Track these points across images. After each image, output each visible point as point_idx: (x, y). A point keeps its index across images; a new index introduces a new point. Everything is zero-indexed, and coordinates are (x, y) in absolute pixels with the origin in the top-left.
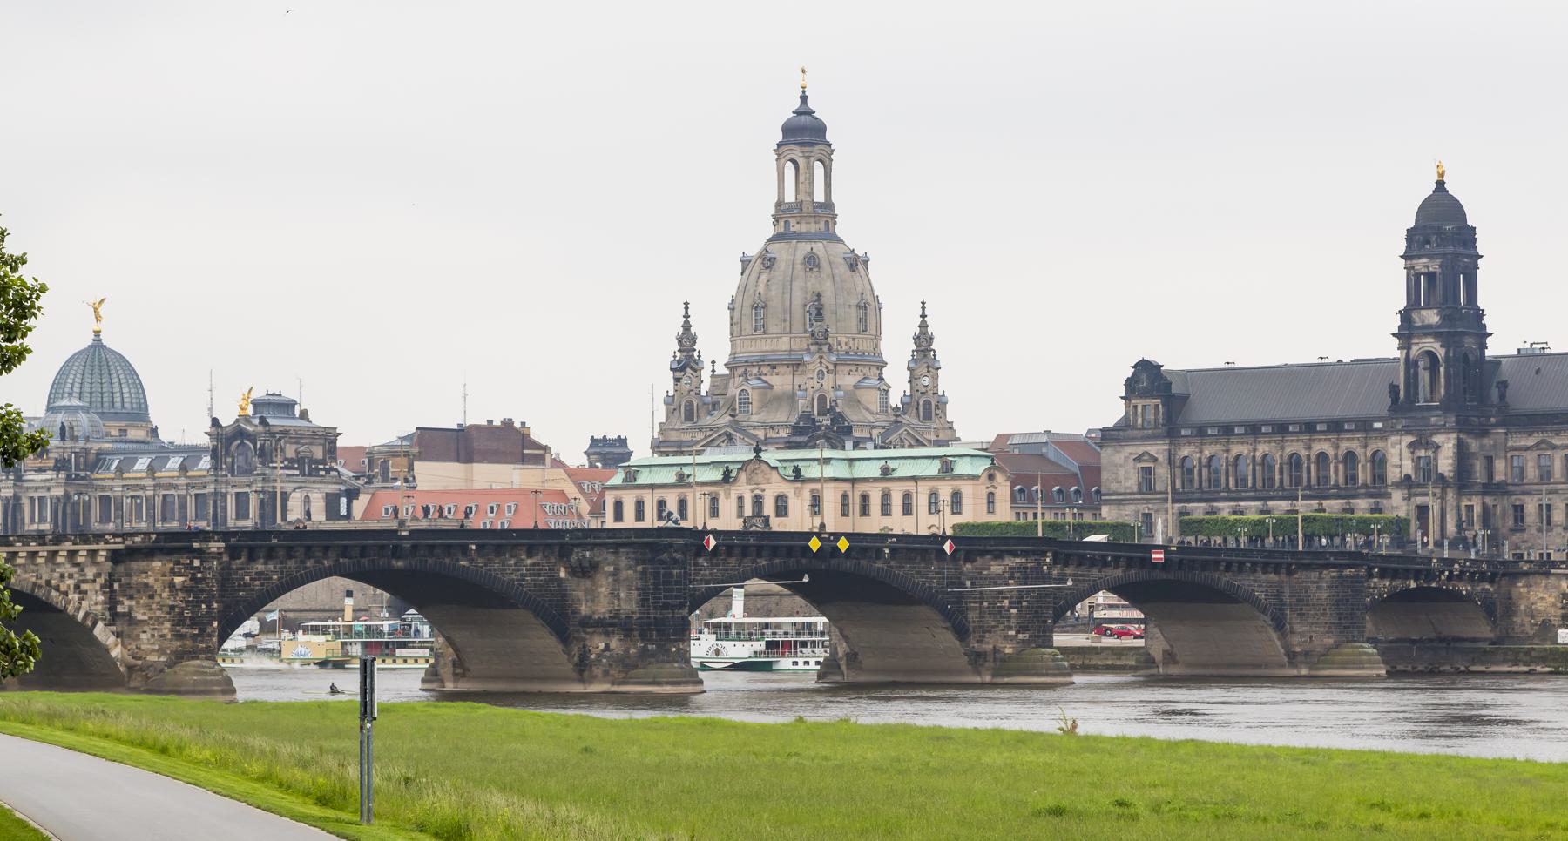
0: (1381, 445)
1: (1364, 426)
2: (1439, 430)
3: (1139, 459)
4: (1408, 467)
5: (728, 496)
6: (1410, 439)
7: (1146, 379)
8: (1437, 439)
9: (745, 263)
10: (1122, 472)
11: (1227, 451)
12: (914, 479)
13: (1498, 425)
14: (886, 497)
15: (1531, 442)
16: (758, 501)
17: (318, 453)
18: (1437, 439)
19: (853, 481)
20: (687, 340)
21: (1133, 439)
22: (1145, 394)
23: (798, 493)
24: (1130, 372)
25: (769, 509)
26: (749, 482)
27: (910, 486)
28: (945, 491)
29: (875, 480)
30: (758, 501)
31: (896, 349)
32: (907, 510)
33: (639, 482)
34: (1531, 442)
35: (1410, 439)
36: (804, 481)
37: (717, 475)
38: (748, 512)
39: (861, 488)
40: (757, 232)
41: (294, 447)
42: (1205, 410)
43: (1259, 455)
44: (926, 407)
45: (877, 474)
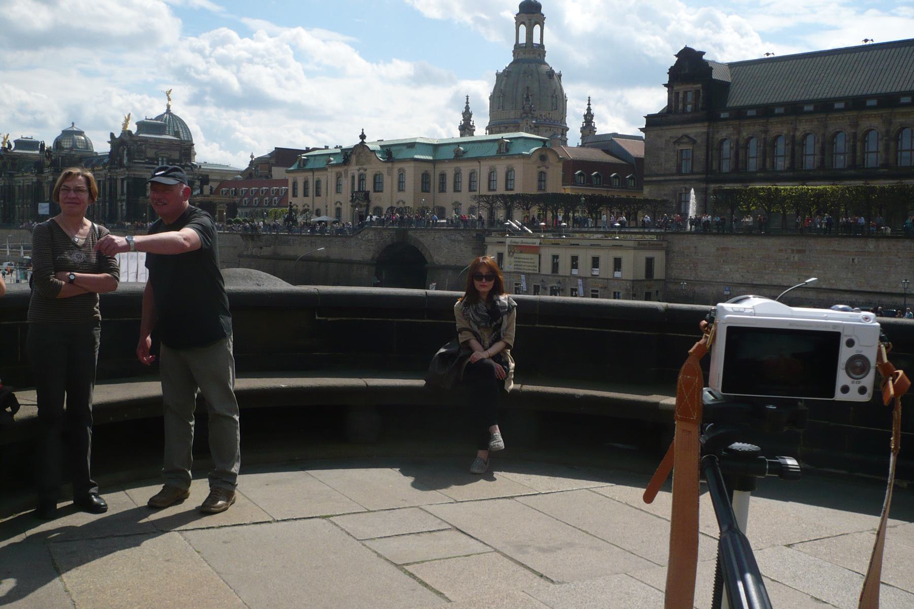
3: (678, 141)
7: (689, 69)
9: (498, 75)
11: (766, 132)
14: (457, 174)
17: (176, 155)
20: (467, 115)
21: (674, 123)
25: (369, 186)
27: (474, 165)
29: (450, 161)
30: (362, 179)
33: (307, 167)
37: (340, 160)
38: (356, 189)
39: (440, 168)
40: (506, 59)
41: (154, 151)
43: (798, 134)
45: (452, 156)
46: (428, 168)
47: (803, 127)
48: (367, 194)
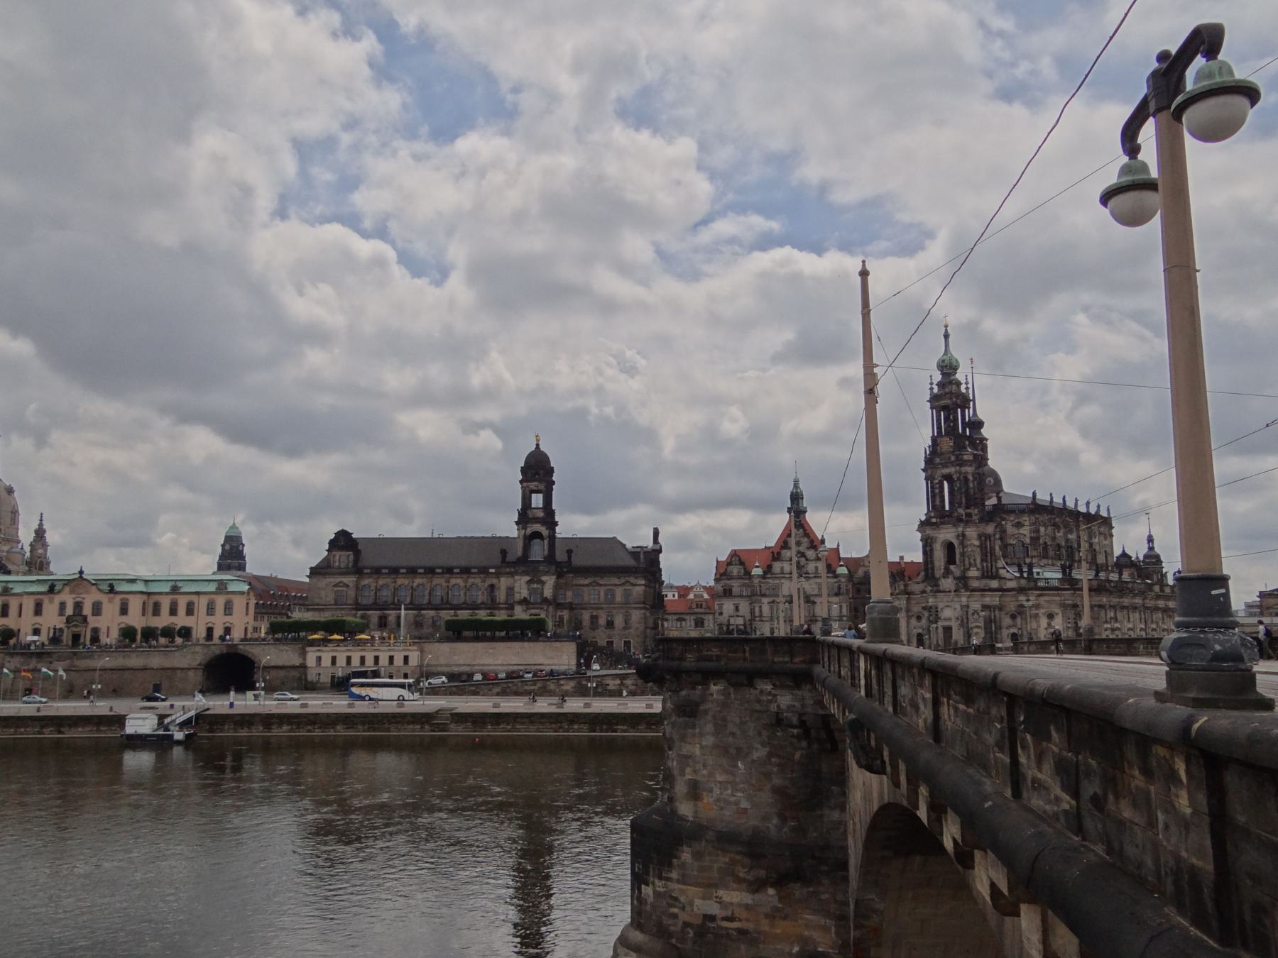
0: (494, 581)
1: (483, 571)
2: (546, 573)
4: (525, 593)
5: (51, 601)
6: (528, 578)
7: (343, 541)
8: (544, 578)
10: (323, 593)
12: (198, 593)
13: (568, 572)
15: (587, 582)
16: (78, 606)
18: (544, 578)
19: (149, 594)
22: (342, 548)
23: (110, 601)
24: (333, 536)
26: (71, 592)
27: (194, 598)
28: (220, 601)
29: (167, 593)
30: (78, 606)
31: (26, 536)
32: (190, 611)
34: (587, 582)
35: (528, 578)
36: (117, 593)
37: (44, 588)
38: (69, 611)
42: (369, 559)
44: (37, 563)
46: (145, 597)
47: (418, 581)
48: (85, 619)
